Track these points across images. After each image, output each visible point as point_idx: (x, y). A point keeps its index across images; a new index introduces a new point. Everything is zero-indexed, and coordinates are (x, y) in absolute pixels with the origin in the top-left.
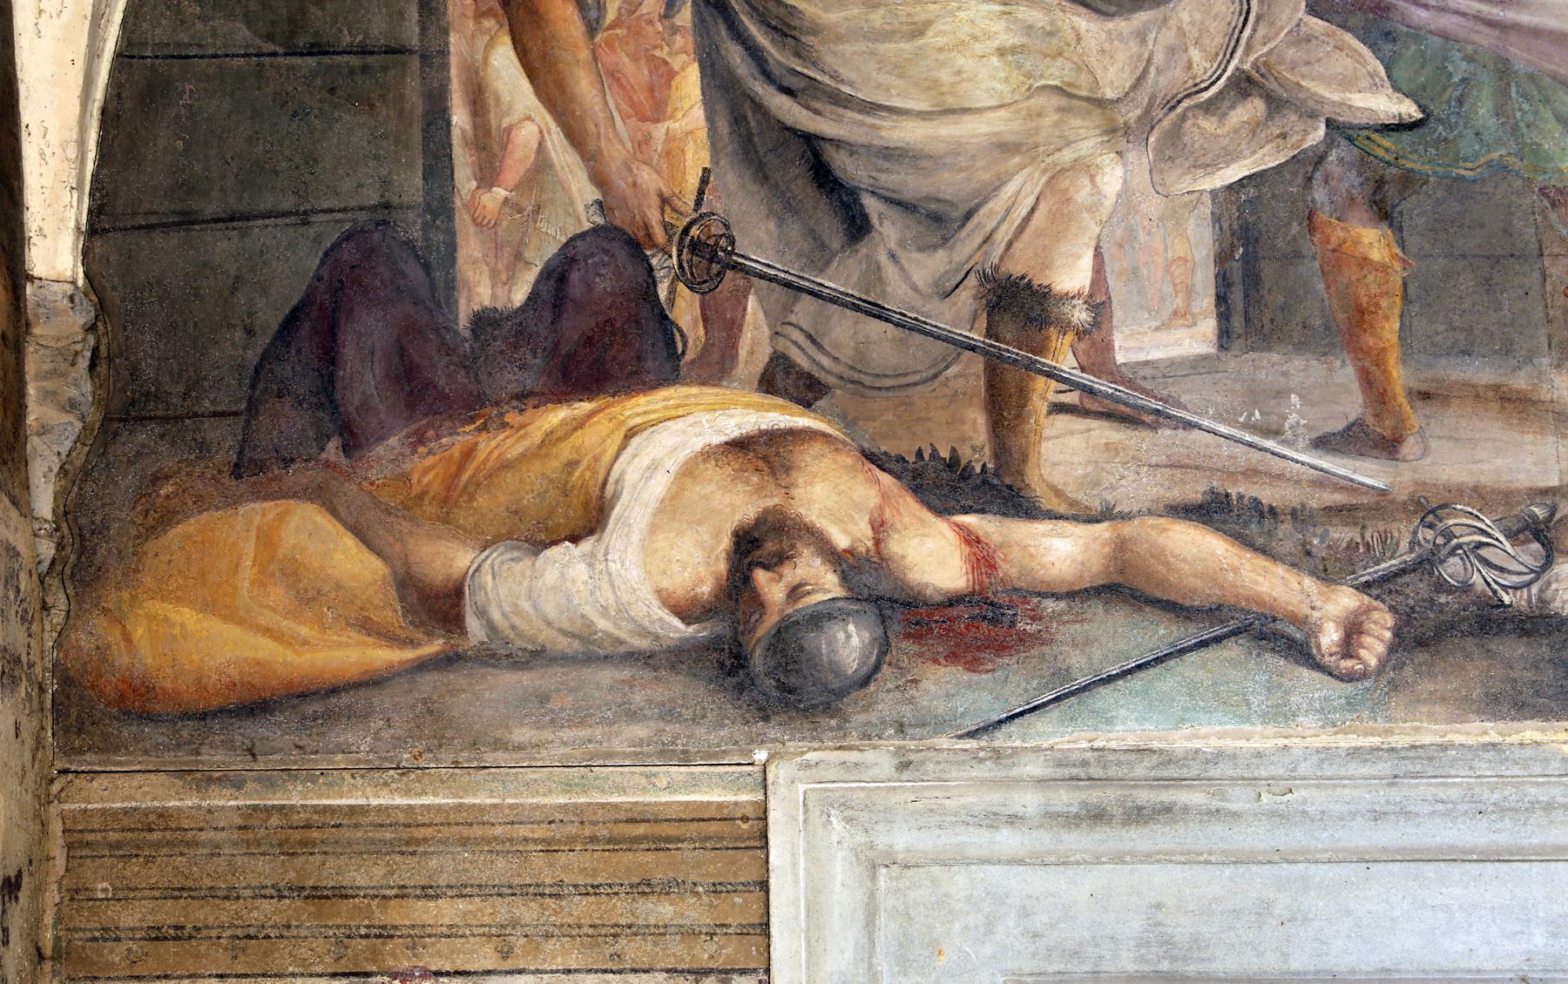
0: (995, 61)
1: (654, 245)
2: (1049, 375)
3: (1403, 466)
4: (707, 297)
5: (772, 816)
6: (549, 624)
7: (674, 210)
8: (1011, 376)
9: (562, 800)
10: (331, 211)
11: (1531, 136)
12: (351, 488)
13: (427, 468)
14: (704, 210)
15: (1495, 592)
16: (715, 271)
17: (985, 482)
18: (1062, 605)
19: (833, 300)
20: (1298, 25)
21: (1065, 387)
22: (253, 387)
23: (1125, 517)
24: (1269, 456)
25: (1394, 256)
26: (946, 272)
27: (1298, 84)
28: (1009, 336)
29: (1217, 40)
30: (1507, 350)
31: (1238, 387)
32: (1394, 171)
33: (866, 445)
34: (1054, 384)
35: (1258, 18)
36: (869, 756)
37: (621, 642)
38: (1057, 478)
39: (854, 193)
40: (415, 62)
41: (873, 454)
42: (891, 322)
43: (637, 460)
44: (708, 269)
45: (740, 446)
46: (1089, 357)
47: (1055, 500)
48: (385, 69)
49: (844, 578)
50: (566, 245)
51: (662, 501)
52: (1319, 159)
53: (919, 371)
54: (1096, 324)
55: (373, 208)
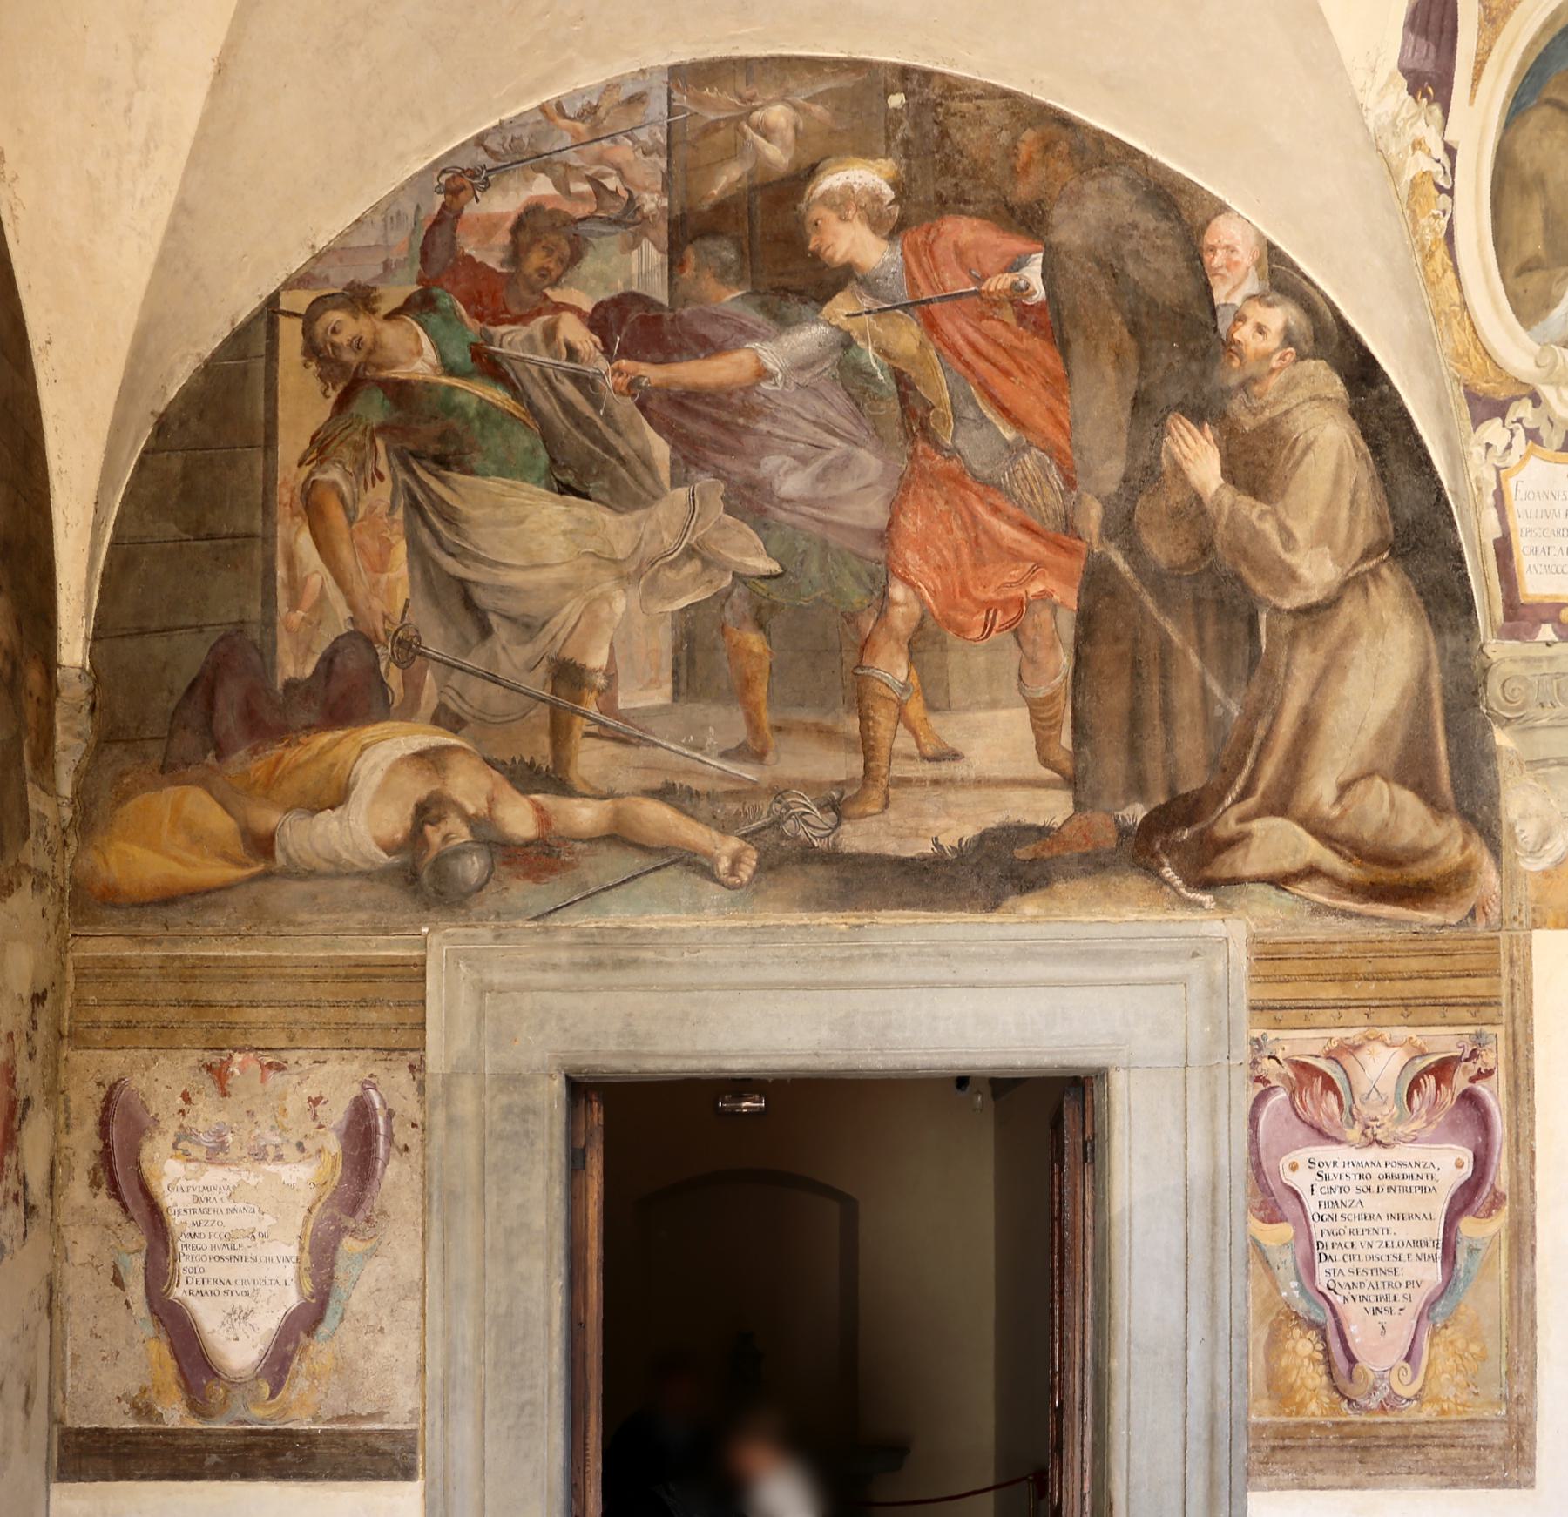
0: (561, 538)
5: (428, 962)
6: (318, 855)
9: (322, 955)
10: (214, 625)
12: (219, 779)
13: (257, 767)
14: (406, 622)
18: (585, 846)
19: (472, 673)
22: (171, 723)
23: (620, 796)
29: (676, 527)
34: (585, 721)
35: (699, 515)
36: (480, 931)
37: (353, 865)
40: (259, 542)
45: (420, 755)
48: (244, 546)
49: (472, 830)
50: (333, 643)
52: (729, 595)
54: (609, 686)
55: (235, 623)
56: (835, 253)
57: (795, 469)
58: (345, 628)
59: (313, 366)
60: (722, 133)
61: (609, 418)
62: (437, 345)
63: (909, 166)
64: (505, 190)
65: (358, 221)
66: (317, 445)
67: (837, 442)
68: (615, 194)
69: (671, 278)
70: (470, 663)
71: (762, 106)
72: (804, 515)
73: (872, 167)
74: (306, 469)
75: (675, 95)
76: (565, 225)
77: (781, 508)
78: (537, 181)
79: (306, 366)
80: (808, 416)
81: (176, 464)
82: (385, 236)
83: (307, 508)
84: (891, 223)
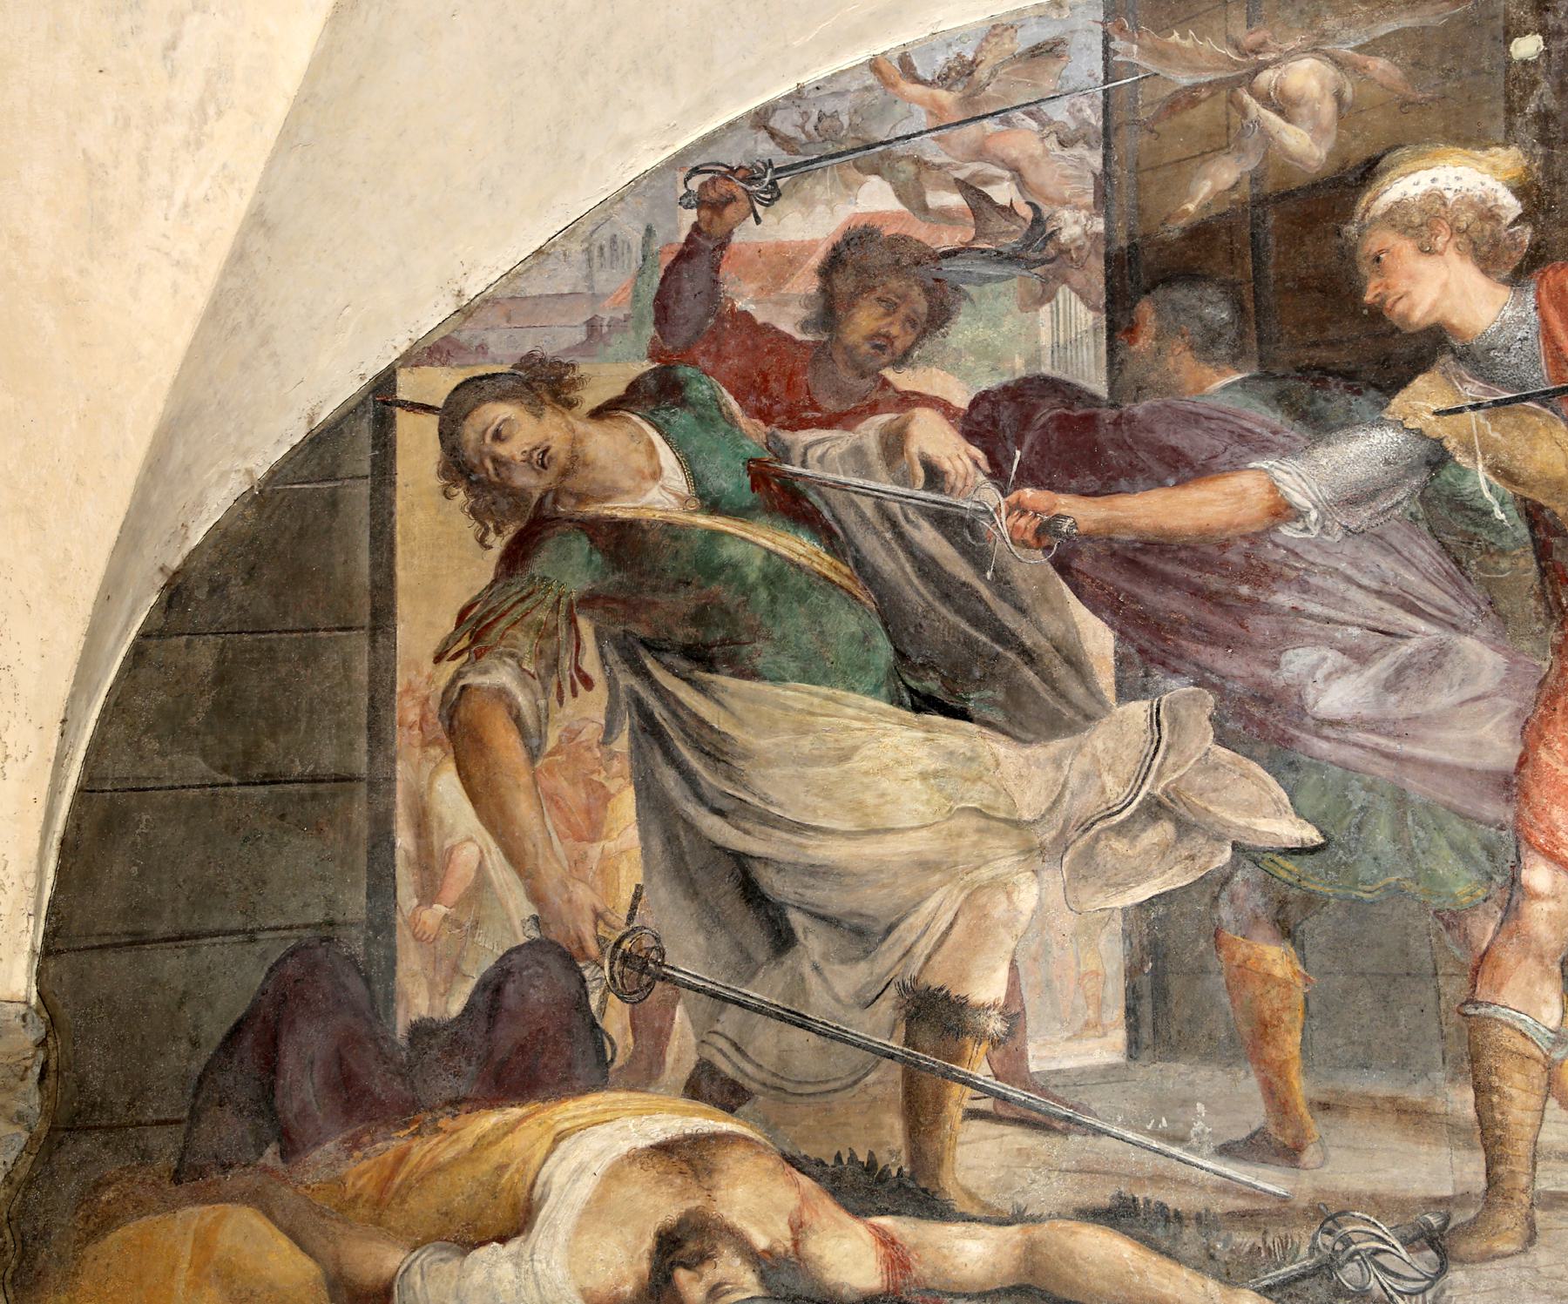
0: (917, 784)
1: (588, 958)
2: (965, 1083)
3: (1303, 1173)
4: (637, 1007)
7: (607, 924)
8: (928, 1084)
10: (277, 929)
11: (1426, 863)
12: (287, 1192)
13: (361, 1172)
14: (636, 924)
15: (1391, 1298)
16: (645, 982)
17: (900, 1185)
19: (758, 1010)
20: (1206, 754)
21: (978, 1094)
22: (195, 1096)
23: (1036, 1220)
24: (1175, 1162)
25: (1295, 973)
26: (868, 983)
27: (1206, 809)
28: (927, 1045)
29: (1129, 767)
30: (1404, 1063)
31: (1146, 1095)
32: (1297, 892)
33: (787, 1149)
34: (969, 1091)
35: (1169, 747)
38: (970, 1181)
39: (780, 908)
40: (363, 789)
41: (794, 1158)
42: (813, 1031)
43: (564, 1163)
44: (639, 980)
45: (664, 1148)
46: (1003, 1065)
47: (968, 1203)
48: (334, 795)
49: (763, 1278)
51: (588, 1203)
52: (1226, 880)
53: (840, 1078)
54: (1010, 1033)
55: (318, 926)
56: (1412, 307)
57: (1345, 670)
58: (523, 934)
59: (460, 496)
60: (1203, 107)
61: (1002, 585)
62: (687, 462)
63: (1548, 158)
64: (809, 203)
65: (539, 252)
66: (468, 626)
67: (1421, 625)
68: (1009, 211)
69: (1112, 351)
70: (755, 993)
71: (1276, 61)
72: (1362, 747)
73: (1479, 160)
74: (449, 668)
75: (1118, 44)
76: (918, 263)
77: (1318, 735)
78: (865, 188)
79: (447, 495)
80: (1365, 581)
81: (204, 656)
82: (589, 277)
83: (451, 731)
84: (1517, 256)
